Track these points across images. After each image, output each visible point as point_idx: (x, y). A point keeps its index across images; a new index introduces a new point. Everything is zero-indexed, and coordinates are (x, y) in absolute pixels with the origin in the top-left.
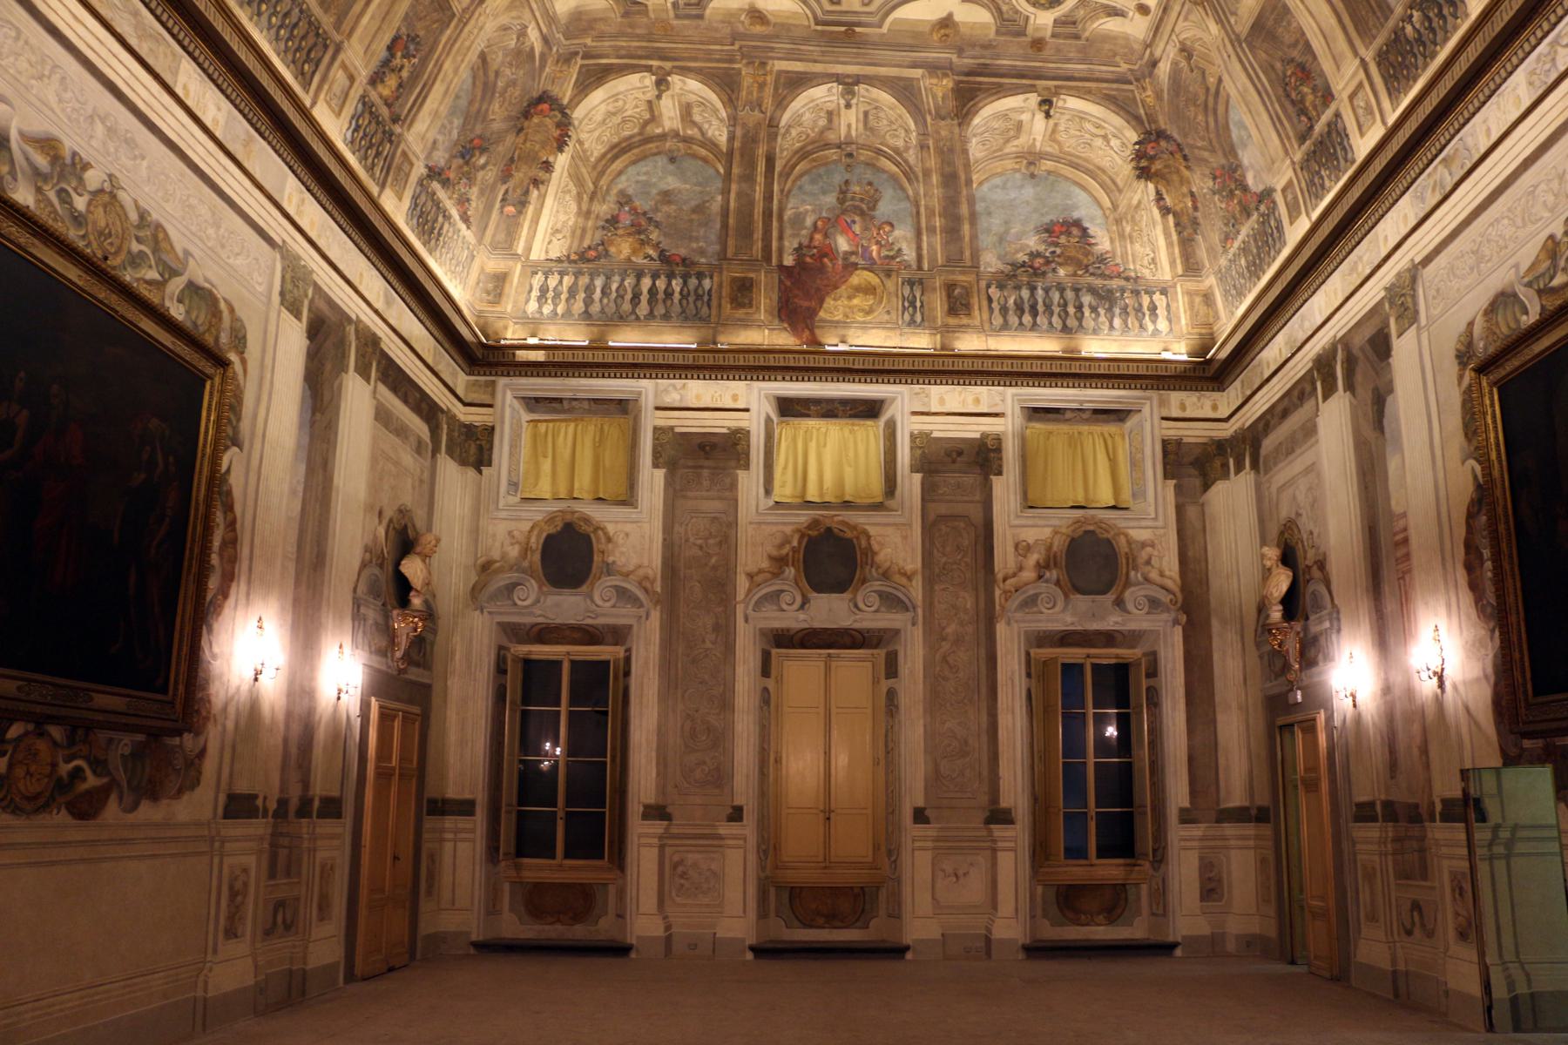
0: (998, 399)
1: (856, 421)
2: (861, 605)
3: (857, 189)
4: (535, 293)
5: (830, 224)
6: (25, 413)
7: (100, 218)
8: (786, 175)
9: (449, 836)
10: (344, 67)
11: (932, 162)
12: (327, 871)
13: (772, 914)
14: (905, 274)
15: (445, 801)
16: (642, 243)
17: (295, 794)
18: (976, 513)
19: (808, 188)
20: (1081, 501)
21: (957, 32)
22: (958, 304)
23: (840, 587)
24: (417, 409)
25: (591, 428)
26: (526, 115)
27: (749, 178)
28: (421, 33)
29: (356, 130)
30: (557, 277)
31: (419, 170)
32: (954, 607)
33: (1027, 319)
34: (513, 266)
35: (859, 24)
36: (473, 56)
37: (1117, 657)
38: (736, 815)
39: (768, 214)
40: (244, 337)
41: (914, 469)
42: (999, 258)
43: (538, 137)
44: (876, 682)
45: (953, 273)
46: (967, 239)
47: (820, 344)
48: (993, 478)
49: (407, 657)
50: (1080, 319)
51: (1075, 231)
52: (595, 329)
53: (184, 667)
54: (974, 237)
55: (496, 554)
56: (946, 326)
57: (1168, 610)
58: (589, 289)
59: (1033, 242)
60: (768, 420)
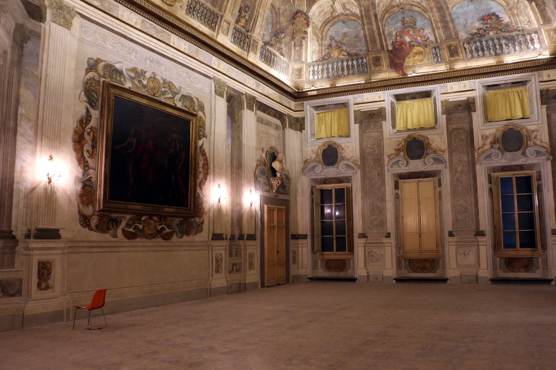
0: (473, 84)
1: (423, 99)
2: (427, 163)
3: (408, 19)
4: (311, 73)
5: (401, 33)
6: (135, 139)
7: (151, 85)
8: (382, 19)
9: (300, 245)
10: (225, 21)
11: (432, 4)
12: (251, 256)
13: (403, 268)
14: (432, 45)
15: (298, 235)
16: (341, 51)
17: (237, 233)
18: (467, 127)
19: (391, 22)
20: (509, 117)
22: (453, 52)
23: (419, 157)
24: (275, 116)
25: (336, 113)
26: (294, 18)
27: (370, 23)
28: (249, 4)
29: (235, 37)
30: (317, 67)
31: (261, 44)
32: (460, 161)
33: (481, 53)
34: (301, 66)
36: (269, 6)
37: (526, 174)
38: (388, 235)
39: (379, 34)
40: (203, 106)
41: (443, 114)
42: (466, 33)
43: (300, 24)
44: (435, 188)
45: (449, 41)
46: (452, 29)
47: (407, 75)
48: (472, 113)
49: (278, 191)
50: (502, 50)
51: (493, 17)
52: (332, 81)
53: (192, 200)
54: (454, 28)
55: (308, 158)
56: (451, 61)
57: (544, 155)
58: (328, 69)
59: (477, 25)
60: (392, 103)
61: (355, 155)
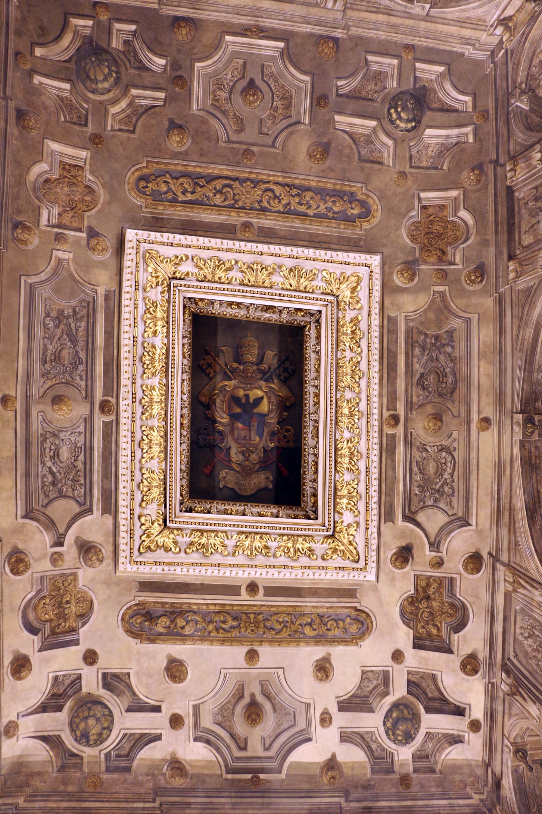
21: (341, 773)
35: (263, 771)
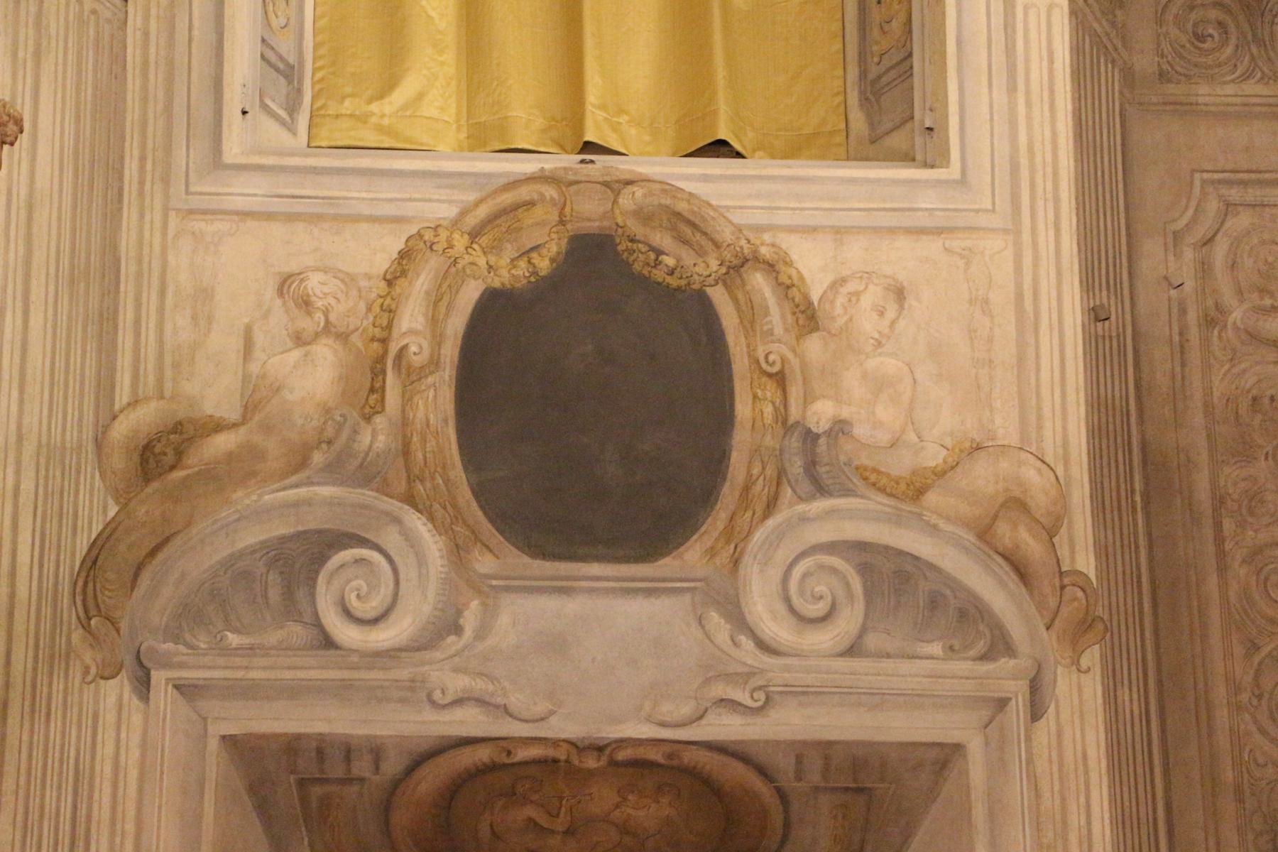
55: (215, 393)
61: (1006, 428)
